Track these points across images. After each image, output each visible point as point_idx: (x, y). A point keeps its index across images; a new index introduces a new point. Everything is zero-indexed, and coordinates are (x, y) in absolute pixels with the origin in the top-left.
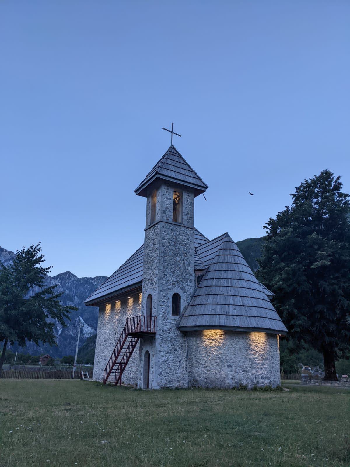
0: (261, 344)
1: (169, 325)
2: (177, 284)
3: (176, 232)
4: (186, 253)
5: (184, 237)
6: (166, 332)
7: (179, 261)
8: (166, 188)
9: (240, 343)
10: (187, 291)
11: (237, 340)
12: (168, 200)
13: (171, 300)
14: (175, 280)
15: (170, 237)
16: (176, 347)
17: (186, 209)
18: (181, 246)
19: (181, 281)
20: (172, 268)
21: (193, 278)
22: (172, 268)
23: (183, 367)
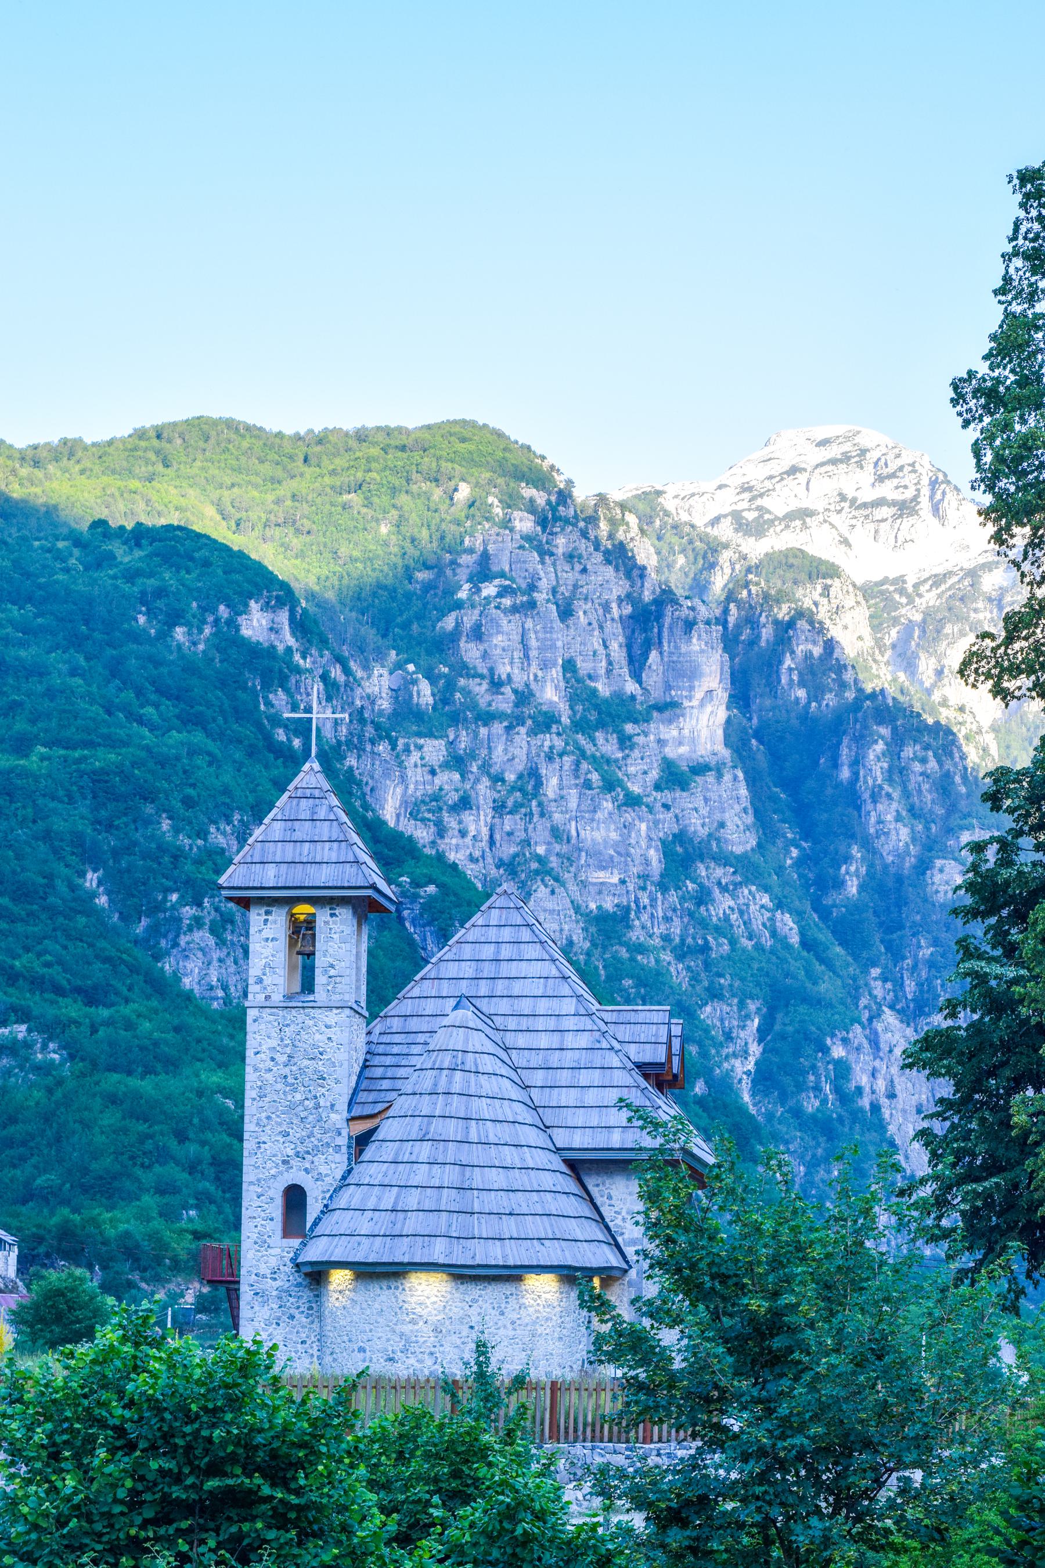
0: (434, 1299)
1: (273, 1262)
2: (295, 1162)
3: (292, 1028)
4: (324, 1079)
5: (318, 1036)
6: (264, 1277)
7: (302, 1102)
8: (262, 911)
9: (383, 1298)
10: (327, 1175)
11: (378, 1291)
12: (270, 944)
13: (279, 1201)
14: (291, 1153)
15: (274, 1043)
16: (292, 1311)
17: (325, 956)
18: (306, 1062)
19: (308, 1153)
20: (280, 1124)
21: (343, 1141)
22: (280, 1124)
23: (312, 1355)
